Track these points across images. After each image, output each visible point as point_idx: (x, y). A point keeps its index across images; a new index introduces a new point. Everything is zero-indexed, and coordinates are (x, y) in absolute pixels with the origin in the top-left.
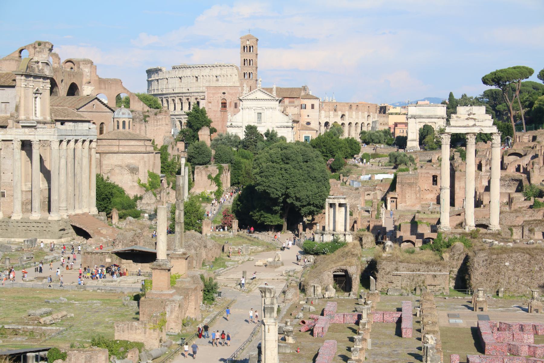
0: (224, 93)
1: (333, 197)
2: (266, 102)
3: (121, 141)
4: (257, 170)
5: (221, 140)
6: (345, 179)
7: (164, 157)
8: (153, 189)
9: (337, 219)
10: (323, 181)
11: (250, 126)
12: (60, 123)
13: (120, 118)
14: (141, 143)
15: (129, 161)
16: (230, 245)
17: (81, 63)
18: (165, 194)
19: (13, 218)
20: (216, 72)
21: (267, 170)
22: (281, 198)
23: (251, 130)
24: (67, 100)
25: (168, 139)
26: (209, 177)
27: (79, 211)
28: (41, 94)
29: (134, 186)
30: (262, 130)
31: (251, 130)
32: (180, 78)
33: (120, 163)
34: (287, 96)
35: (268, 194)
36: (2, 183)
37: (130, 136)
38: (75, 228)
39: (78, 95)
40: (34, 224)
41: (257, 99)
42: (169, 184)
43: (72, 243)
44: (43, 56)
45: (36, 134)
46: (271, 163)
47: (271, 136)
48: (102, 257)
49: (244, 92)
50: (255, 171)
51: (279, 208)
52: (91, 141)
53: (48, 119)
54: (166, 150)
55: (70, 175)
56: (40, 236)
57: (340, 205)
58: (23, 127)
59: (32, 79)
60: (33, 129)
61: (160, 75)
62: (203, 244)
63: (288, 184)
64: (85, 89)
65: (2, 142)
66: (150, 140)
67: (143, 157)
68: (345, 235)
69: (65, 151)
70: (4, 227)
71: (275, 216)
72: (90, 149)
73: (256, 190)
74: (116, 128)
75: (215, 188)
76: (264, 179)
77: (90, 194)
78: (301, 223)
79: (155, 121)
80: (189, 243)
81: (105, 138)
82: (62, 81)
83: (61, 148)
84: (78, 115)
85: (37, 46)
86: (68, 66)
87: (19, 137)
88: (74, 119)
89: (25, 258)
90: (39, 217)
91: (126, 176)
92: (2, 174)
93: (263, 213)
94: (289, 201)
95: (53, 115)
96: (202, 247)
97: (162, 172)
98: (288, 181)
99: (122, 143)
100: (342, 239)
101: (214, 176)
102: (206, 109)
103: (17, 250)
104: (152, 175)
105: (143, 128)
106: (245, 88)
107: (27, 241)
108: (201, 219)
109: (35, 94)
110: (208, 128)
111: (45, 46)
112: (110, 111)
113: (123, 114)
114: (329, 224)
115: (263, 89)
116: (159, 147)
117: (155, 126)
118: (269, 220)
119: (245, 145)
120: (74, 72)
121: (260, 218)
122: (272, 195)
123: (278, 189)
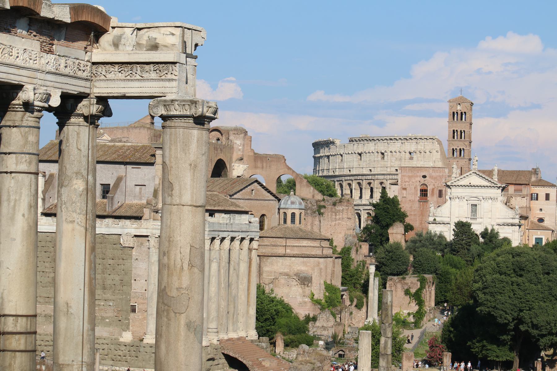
0: (424, 177)
2: (483, 190)
3: (288, 241)
4: (479, 285)
5: (420, 241)
7: (345, 263)
8: (331, 308)
11: (462, 222)
13: (288, 209)
14: (316, 243)
15: (298, 268)
17: (231, 133)
18: (347, 314)
19: (145, 341)
20: (411, 146)
23: (463, 228)
24: (216, 183)
25: (351, 238)
26: (407, 292)
27: (233, 335)
29: (305, 302)
30: (477, 229)
31: (463, 228)
33: (286, 270)
34: (514, 181)
35: (494, 318)
36: (132, 294)
37: (301, 233)
39: (227, 176)
42: (352, 301)
46: (498, 276)
47: (490, 236)
49: (454, 175)
50: (477, 285)
51: (509, 337)
52: (252, 240)
54: (349, 254)
55: (223, 285)
61: (333, 150)
63: (521, 305)
64: (235, 167)
65: (135, 238)
67: (319, 263)
70: (133, 353)
71: (503, 348)
72: (250, 250)
73: (477, 311)
74: (282, 222)
75: (414, 308)
76: (489, 298)
77: (248, 312)
78: (540, 359)
79: (334, 214)
81: (268, 235)
84: (233, 204)
86: (214, 137)
88: (227, 209)
92: (133, 281)
94: (522, 328)
97: (343, 284)
98: (522, 300)
99: (290, 242)
101: (413, 291)
102: (399, 198)
104: (329, 288)
105: (317, 222)
106: (454, 170)
112: (274, 198)
113: (293, 203)
115: (479, 171)
116: (339, 249)
117: (332, 221)
119: (452, 248)
121: (481, 351)
122: (500, 320)
123: (508, 311)
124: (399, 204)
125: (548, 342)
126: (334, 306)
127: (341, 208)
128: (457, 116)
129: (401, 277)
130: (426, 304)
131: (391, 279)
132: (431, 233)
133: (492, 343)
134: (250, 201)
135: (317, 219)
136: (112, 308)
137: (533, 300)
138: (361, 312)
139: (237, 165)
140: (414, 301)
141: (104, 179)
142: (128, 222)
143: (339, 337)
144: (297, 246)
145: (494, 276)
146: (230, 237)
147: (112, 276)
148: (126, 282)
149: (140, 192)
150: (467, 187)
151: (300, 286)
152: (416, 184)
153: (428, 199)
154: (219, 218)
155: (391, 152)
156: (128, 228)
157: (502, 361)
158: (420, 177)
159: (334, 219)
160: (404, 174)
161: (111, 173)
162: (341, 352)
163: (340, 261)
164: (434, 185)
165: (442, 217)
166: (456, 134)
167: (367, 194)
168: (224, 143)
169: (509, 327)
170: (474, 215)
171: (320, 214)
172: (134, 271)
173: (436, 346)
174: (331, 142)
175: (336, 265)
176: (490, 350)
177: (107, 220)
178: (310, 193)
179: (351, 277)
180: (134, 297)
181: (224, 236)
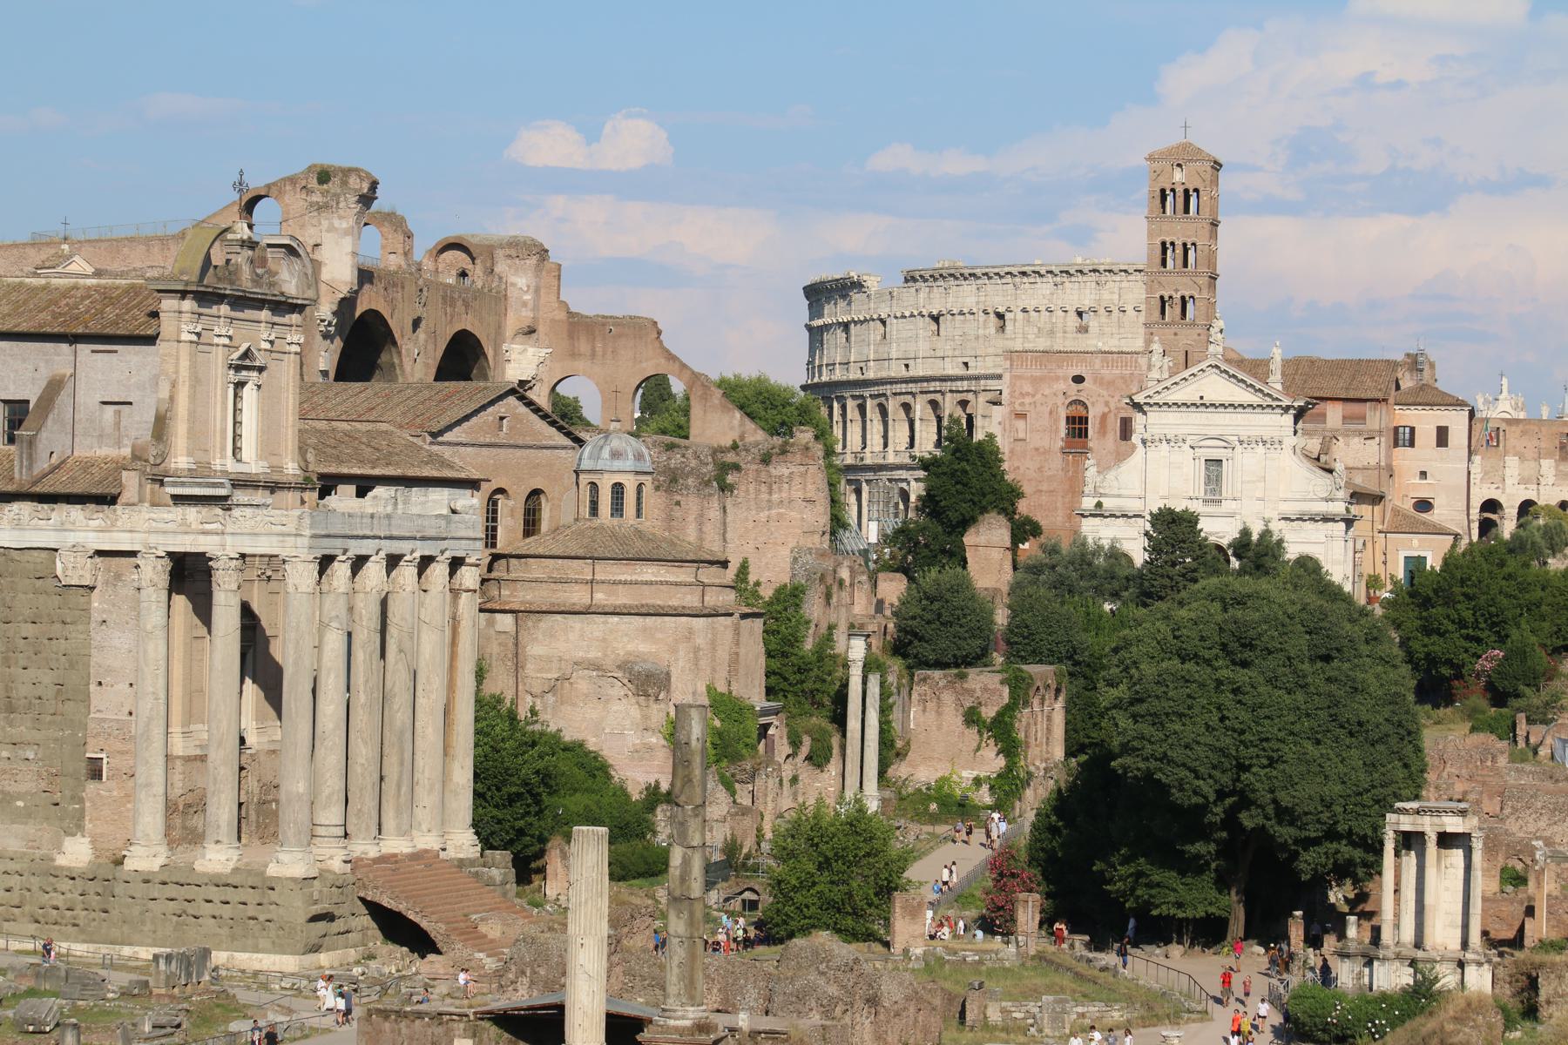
0: (1078, 379)
1: (1414, 805)
2: (1240, 418)
3: (599, 566)
4: (1122, 691)
5: (1053, 567)
6: (1537, 733)
8: (724, 763)
9: (1429, 899)
10: (1393, 740)
11: (1171, 512)
12: (352, 489)
13: (600, 472)
14: (685, 574)
15: (630, 647)
16: (992, 996)
18: (772, 783)
19: (130, 865)
20: (1080, 294)
21: (1160, 690)
22: (1218, 810)
24: (396, 400)
25: (809, 559)
26: (971, 717)
27: (395, 845)
28: (261, 369)
29: (650, 748)
30: (1218, 529)
31: (1173, 529)
32: (936, 319)
33: (594, 654)
34: (1325, 393)
35: (1163, 789)
36: (91, 725)
37: (639, 543)
38: (376, 911)
39: (485, 378)
40: (213, 893)
41: (1202, 405)
42: (795, 743)
43: (357, 971)
45: (229, 529)
46: (1176, 661)
47: (1257, 553)
48: (440, 1030)
49: (1155, 374)
50: (1114, 692)
51: (1212, 847)
52: (456, 563)
53: (291, 469)
55: (362, 698)
56: (233, 938)
57: (1446, 840)
58: (178, 499)
59: (224, 309)
60: (218, 511)
61: (858, 307)
62: (861, 991)
64: (513, 356)
65: (98, 560)
66: (724, 564)
67: (691, 631)
68: (1461, 964)
69: (342, 602)
70: (94, 900)
72: (455, 593)
73: (1114, 771)
74: (585, 511)
75: (992, 762)
78: (1298, 913)
79: (764, 488)
80: (798, 985)
81: (541, 551)
82: (416, 323)
83: (325, 587)
84: (433, 459)
85: (313, 183)
86: (451, 265)
87: (160, 539)
88: (411, 472)
89: (147, 1028)
90: (231, 865)
91: (616, 707)
92: (93, 687)
93: (1147, 868)
94: (1248, 820)
95: (310, 457)
96: (859, 1004)
97: (770, 692)
98: (1247, 737)
99: (605, 571)
100: (1447, 978)
101: (989, 713)
103: (125, 994)
104: (724, 705)
105: (714, 513)
107: (169, 958)
108: (887, 889)
109: (238, 368)
110: (1002, 519)
111: (344, 183)
112: (567, 442)
113: (616, 455)
114: (1397, 915)
115: (1228, 361)
116: (767, 593)
117: (760, 509)
118: (1172, 898)
119: (1146, 587)
120: (467, 290)
121: (1133, 890)
122: (1176, 794)
123: (1202, 770)
124: (1001, 461)
125: (1323, 860)
126: (735, 758)
127: (786, 472)
128: (1175, 200)
129: (955, 671)
130: (1034, 752)
131: (924, 680)
132: (1084, 544)
133: (1164, 864)
134: (494, 451)
135: (715, 503)
137: (1281, 735)
138: (825, 775)
139: (516, 347)
140: (991, 742)
141: (12, 387)
142: (76, 512)
143: (745, 850)
144: (625, 583)
145: (1164, 665)
146: (382, 554)
147: (31, 672)
148: (72, 690)
149: (117, 424)
150: (1193, 409)
151: (633, 700)
152: (1054, 399)
153: (1090, 444)
154: (344, 499)
155: (1024, 310)
156: (78, 530)
157: (1195, 921)
158: (1065, 379)
159: (764, 504)
160: (1019, 372)
161: (31, 367)
162: (748, 895)
163: (758, 624)
164: (1107, 404)
165: (1119, 496)
166: (1169, 252)
167: (900, 434)
168: (479, 284)
169: (1209, 818)
170: (1213, 491)
171: (725, 488)
172: (96, 658)
173: (1013, 875)
174: (853, 283)
175: (744, 638)
176: (1158, 885)
178: (732, 428)
179: (799, 671)
180: (98, 734)
181: (364, 552)
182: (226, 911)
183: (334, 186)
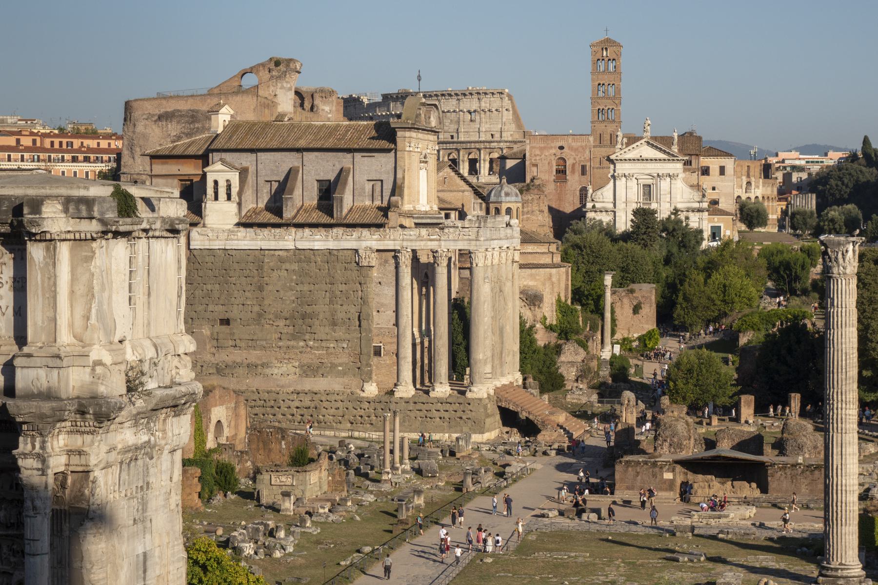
0: (561, 148)
15: (525, 283)
17: (316, 96)
19: (397, 395)
20: (472, 104)
23: (643, 216)
36: (375, 331)
44: (285, 85)
56: (450, 427)
60: (437, 230)
67: (551, 275)
85: (272, 66)
87: (409, 244)
92: (375, 313)
136: (347, 351)
142: (365, 232)
147: (345, 307)
156: (367, 242)
158: (555, 148)
160: (534, 145)
164: (575, 159)
170: (646, 199)
177: (335, 230)
180: (378, 335)
182: (446, 415)
183: (282, 67)
